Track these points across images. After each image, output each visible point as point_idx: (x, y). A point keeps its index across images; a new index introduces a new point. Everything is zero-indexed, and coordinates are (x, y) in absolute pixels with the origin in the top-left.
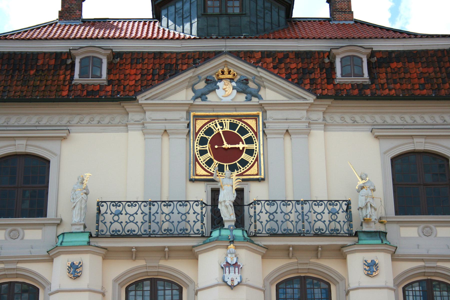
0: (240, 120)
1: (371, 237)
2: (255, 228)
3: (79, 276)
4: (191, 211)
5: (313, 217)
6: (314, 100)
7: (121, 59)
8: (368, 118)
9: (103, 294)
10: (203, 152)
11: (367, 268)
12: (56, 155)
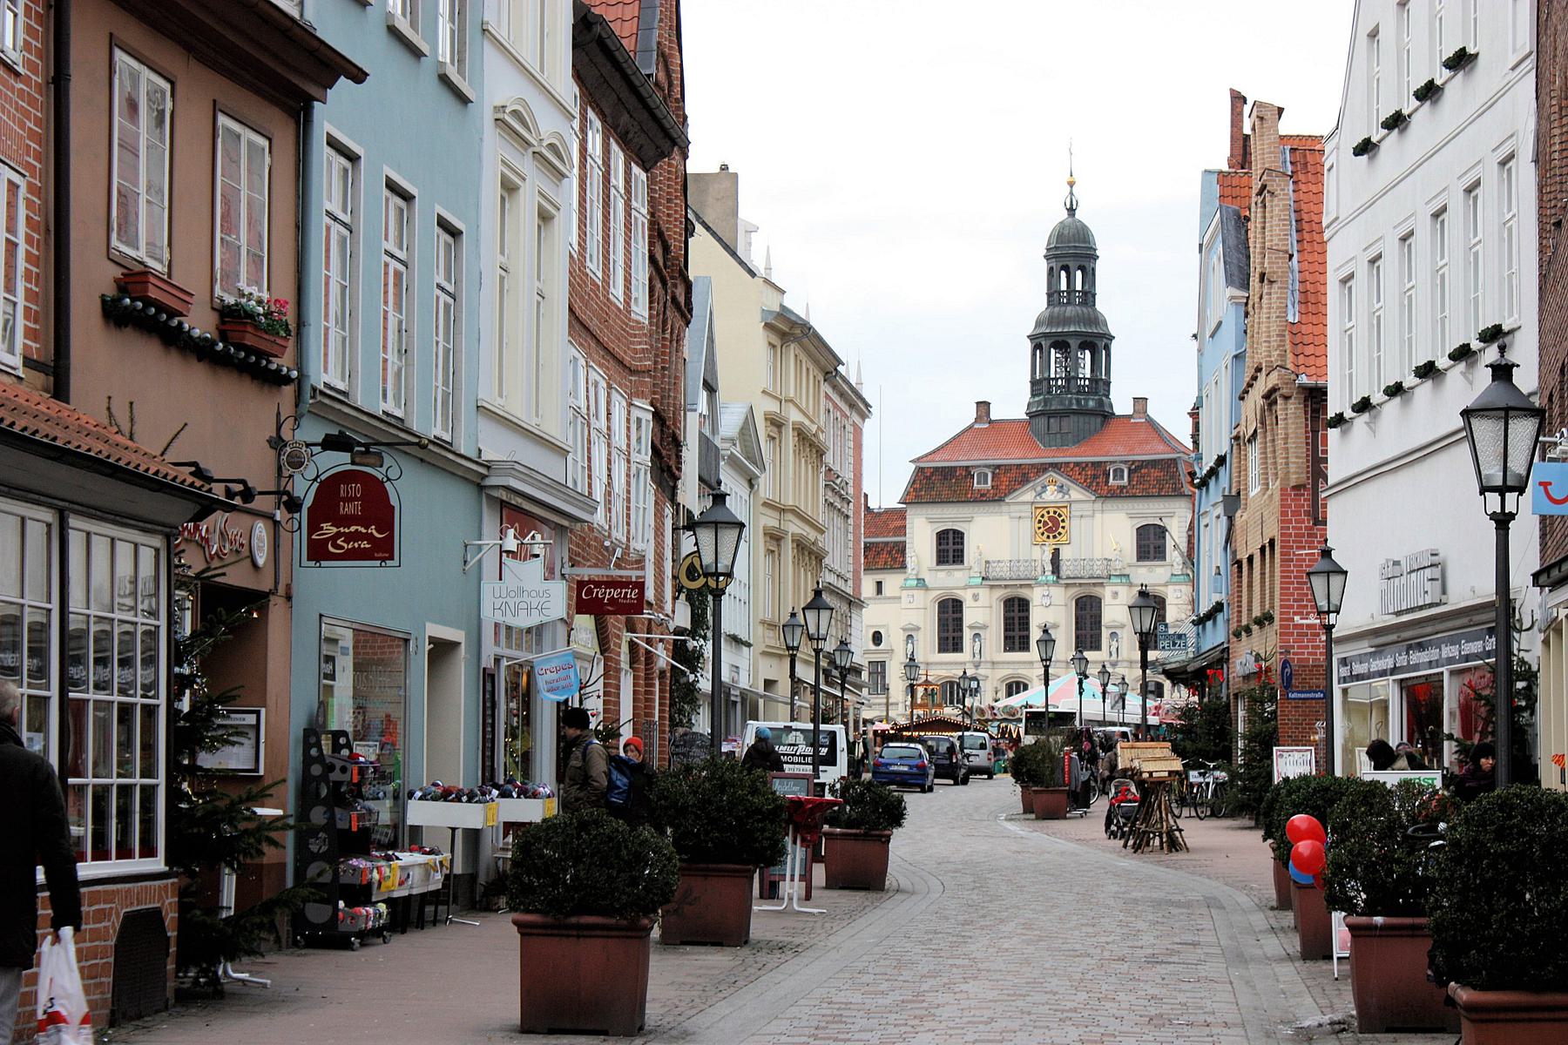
5: (1088, 567)
10: (1039, 528)
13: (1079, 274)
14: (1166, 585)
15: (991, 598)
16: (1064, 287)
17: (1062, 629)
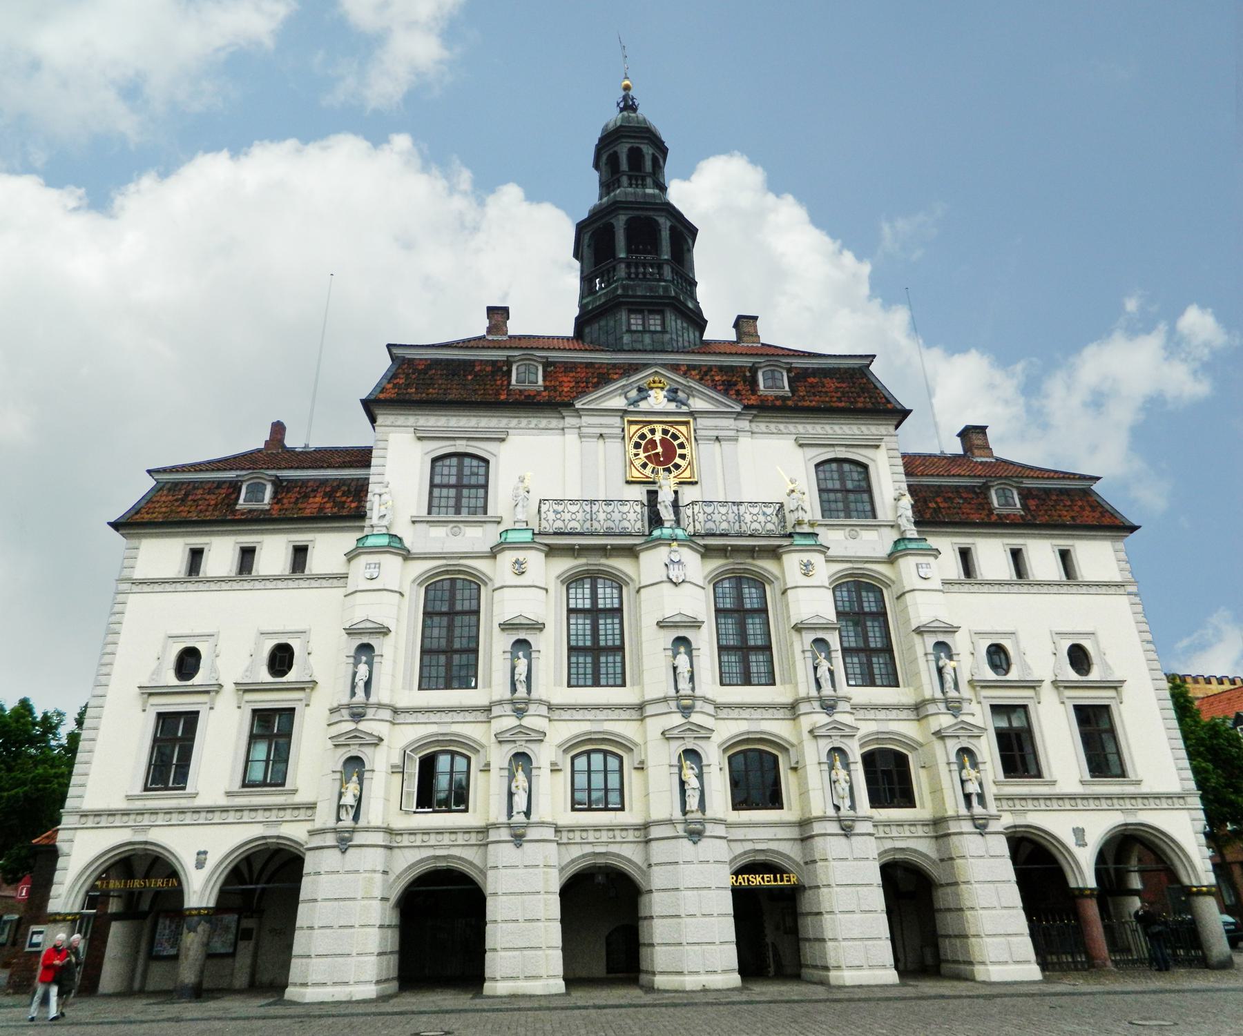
0: (672, 426)
1: (805, 538)
2: (694, 527)
3: (523, 573)
4: (632, 511)
6: (742, 409)
7: (555, 368)
8: (791, 428)
9: (547, 590)
11: (804, 568)
12: (495, 456)
14: (891, 559)
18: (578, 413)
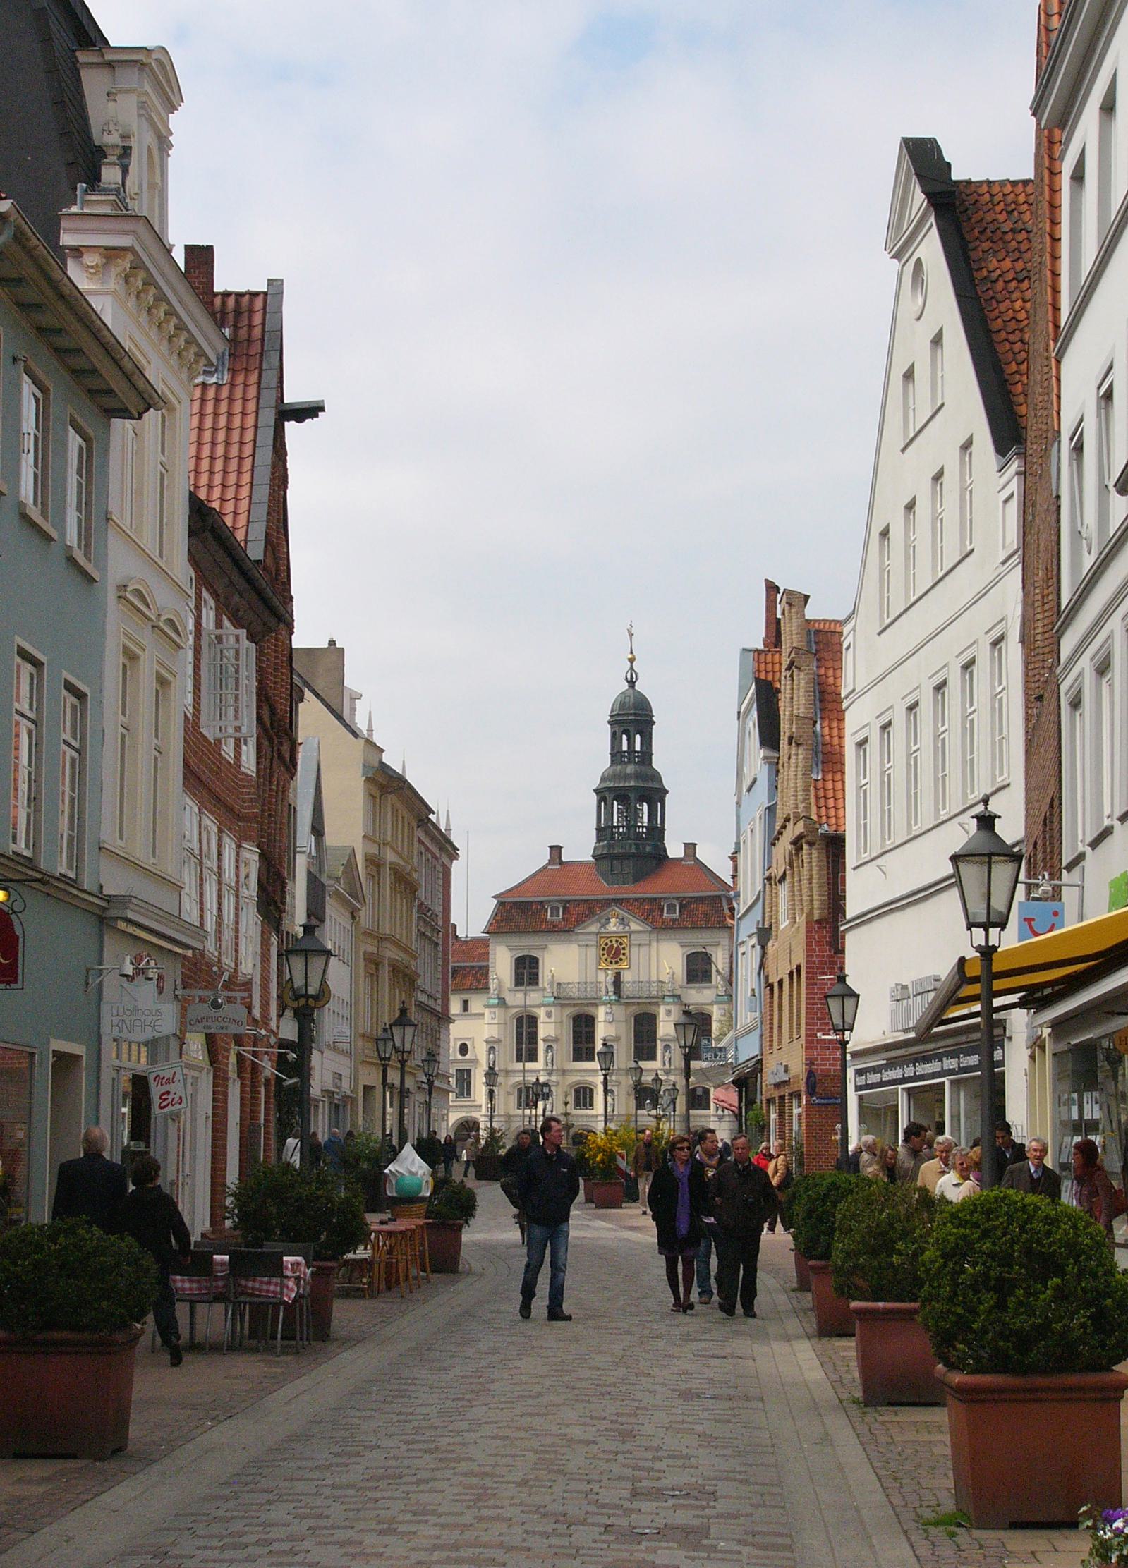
5: (645, 989)
13: (638, 737)
14: (712, 1004)
15: (562, 1015)
16: (625, 748)
17: (623, 1040)
18: (578, 934)
